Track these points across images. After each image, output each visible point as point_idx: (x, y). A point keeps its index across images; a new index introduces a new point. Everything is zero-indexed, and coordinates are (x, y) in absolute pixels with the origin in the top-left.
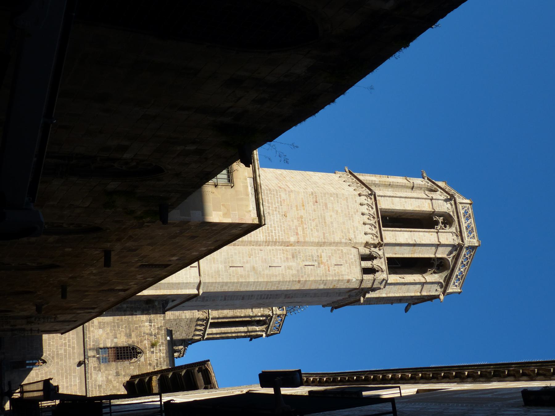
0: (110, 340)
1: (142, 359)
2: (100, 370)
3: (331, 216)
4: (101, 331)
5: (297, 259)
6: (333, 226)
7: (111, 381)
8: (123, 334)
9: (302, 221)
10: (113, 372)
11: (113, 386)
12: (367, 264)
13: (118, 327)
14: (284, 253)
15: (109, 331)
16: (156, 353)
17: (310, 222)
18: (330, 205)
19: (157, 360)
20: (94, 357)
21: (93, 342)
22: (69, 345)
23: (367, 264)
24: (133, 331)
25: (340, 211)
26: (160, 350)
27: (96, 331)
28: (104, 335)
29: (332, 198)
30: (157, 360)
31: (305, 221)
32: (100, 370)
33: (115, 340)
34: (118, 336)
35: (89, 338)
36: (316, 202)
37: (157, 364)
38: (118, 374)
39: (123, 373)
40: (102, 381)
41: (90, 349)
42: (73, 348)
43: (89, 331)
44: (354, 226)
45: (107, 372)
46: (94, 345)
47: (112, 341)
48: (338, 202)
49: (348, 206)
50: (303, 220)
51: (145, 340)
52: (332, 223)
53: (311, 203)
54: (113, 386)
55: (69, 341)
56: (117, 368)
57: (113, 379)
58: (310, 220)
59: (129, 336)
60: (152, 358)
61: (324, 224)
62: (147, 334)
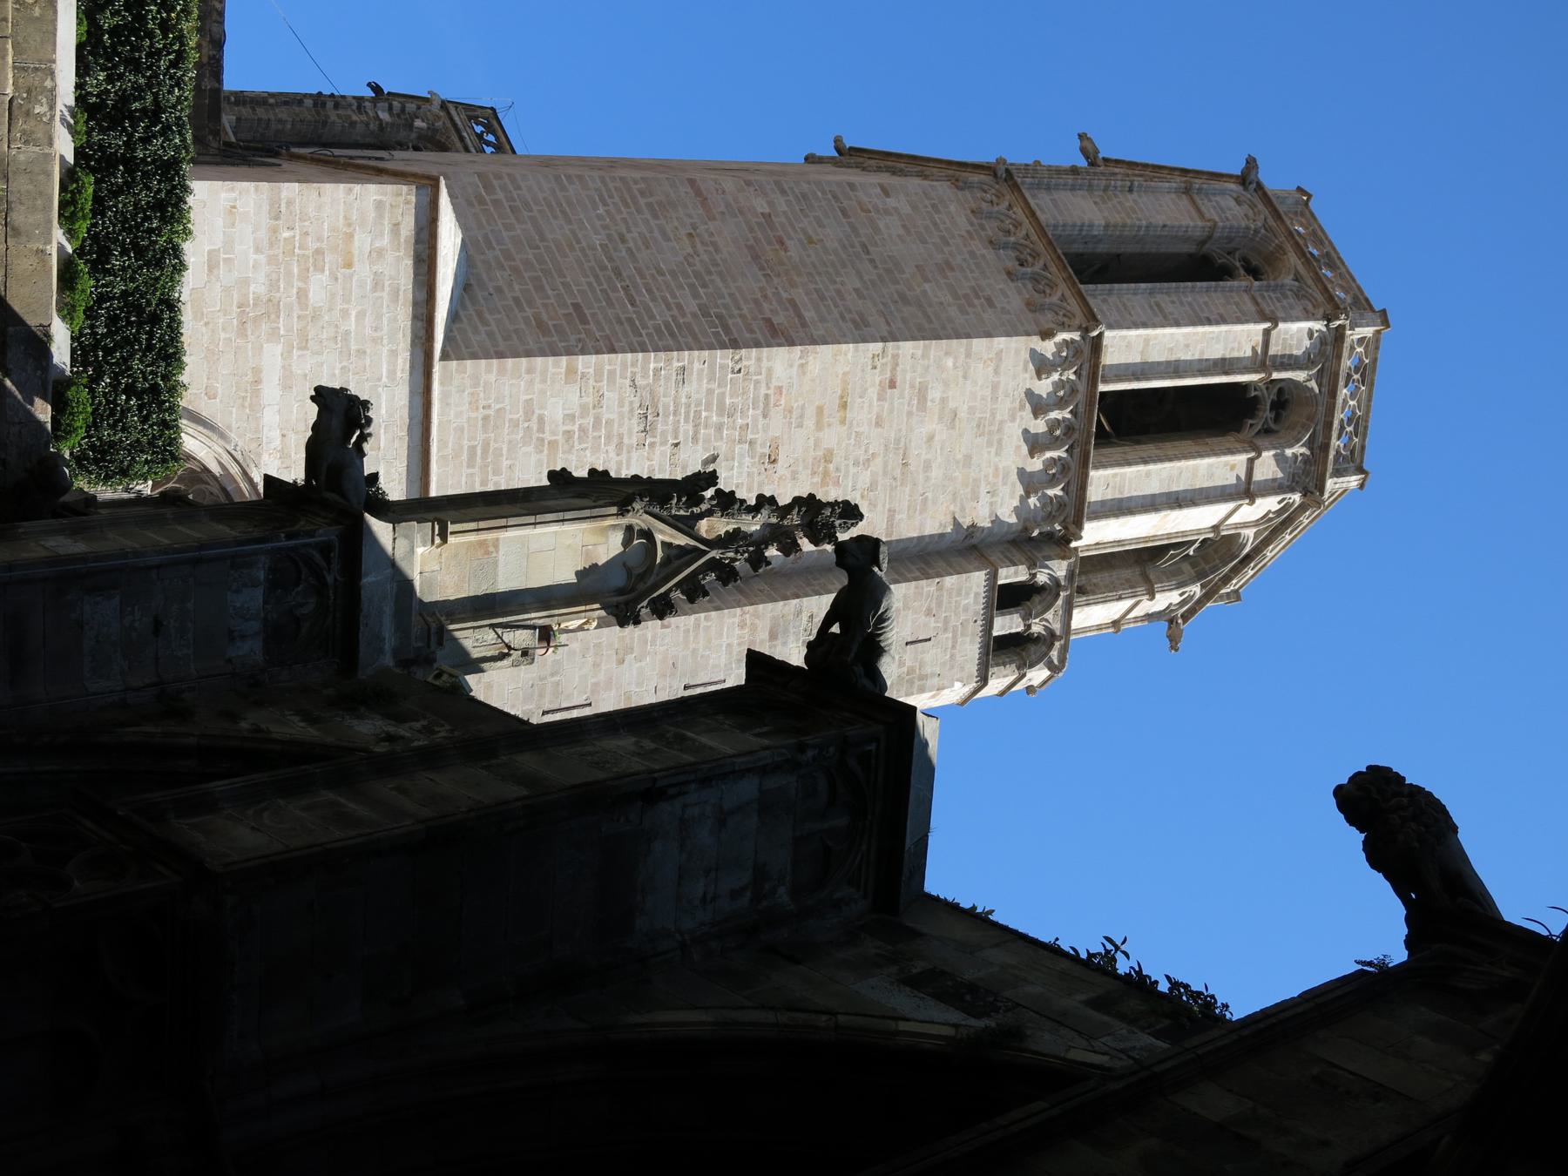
3: (931, 438)
5: (785, 644)
6: (927, 479)
9: (826, 474)
12: (1007, 624)
14: (742, 626)
17: (853, 470)
18: (935, 394)
23: (1007, 624)
25: (963, 414)
29: (950, 363)
31: (838, 470)
36: (892, 385)
44: (997, 469)
48: (965, 377)
49: (995, 387)
50: (831, 467)
52: (927, 466)
53: (873, 393)
58: (856, 464)
61: (898, 473)
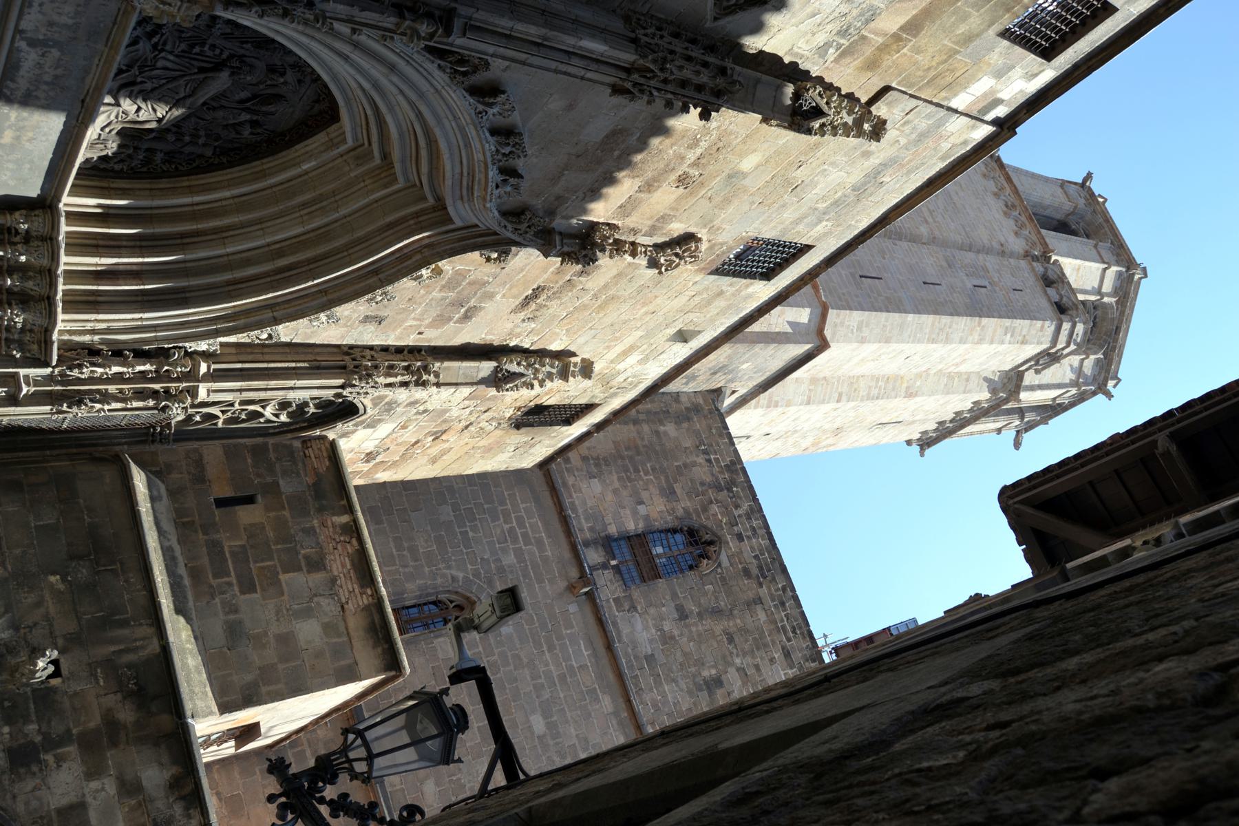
0: (628, 512)
1: (724, 558)
2: (633, 608)
4: (596, 485)
7: (672, 638)
8: (654, 491)
10: (669, 610)
11: (685, 654)
13: (637, 471)
15: (617, 484)
16: (748, 537)
19: (756, 557)
20: (605, 566)
21: (587, 519)
22: (525, 535)
24: (676, 481)
26: (753, 529)
27: (584, 486)
28: (609, 496)
30: (756, 557)
32: (633, 608)
33: (642, 509)
34: (645, 495)
35: (574, 510)
37: (760, 568)
38: (683, 615)
39: (695, 610)
40: (651, 641)
41: (587, 544)
42: (539, 543)
43: (565, 484)
45: (652, 611)
46: (591, 529)
47: (635, 513)
51: (711, 502)
54: (685, 654)
55: (521, 523)
56: (674, 596)
57: (676, 632)
59: (669, 493)
60: (745, 555)
62: (710, 486)
